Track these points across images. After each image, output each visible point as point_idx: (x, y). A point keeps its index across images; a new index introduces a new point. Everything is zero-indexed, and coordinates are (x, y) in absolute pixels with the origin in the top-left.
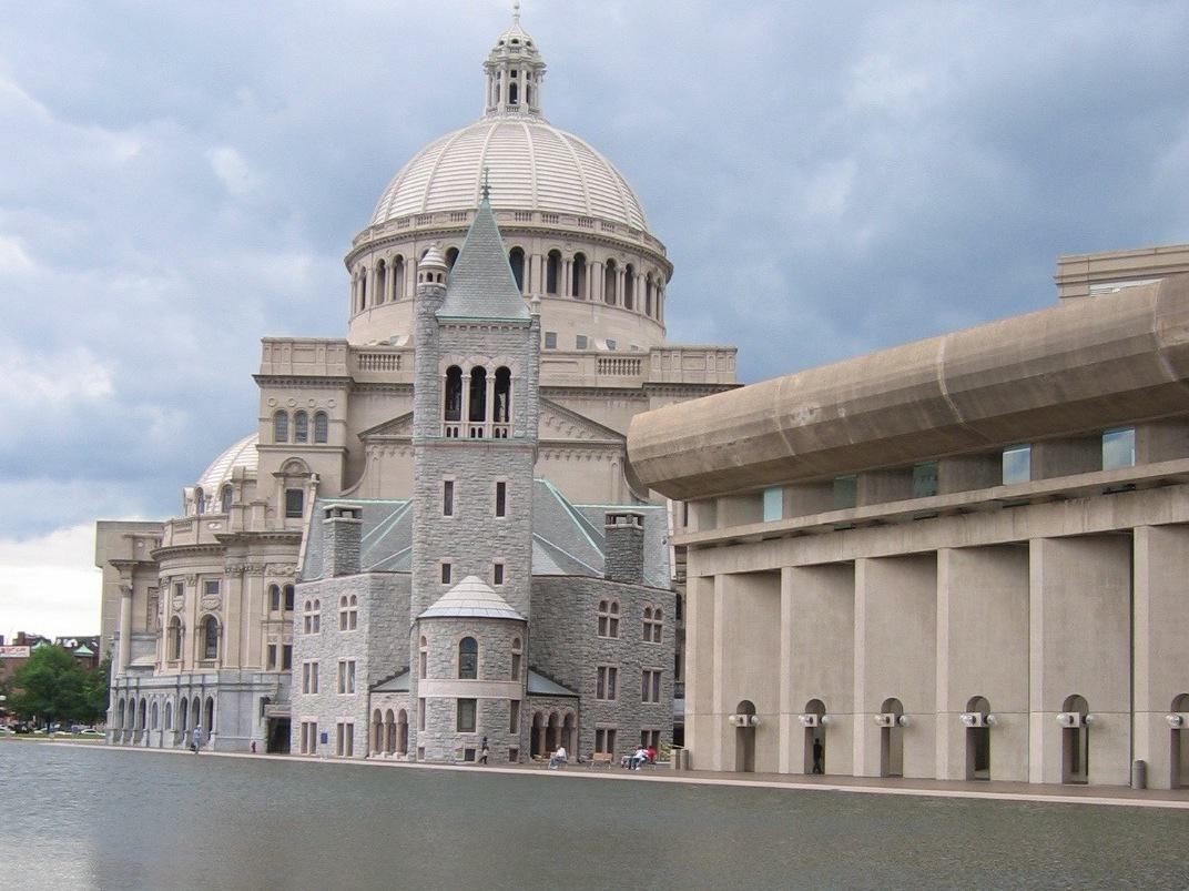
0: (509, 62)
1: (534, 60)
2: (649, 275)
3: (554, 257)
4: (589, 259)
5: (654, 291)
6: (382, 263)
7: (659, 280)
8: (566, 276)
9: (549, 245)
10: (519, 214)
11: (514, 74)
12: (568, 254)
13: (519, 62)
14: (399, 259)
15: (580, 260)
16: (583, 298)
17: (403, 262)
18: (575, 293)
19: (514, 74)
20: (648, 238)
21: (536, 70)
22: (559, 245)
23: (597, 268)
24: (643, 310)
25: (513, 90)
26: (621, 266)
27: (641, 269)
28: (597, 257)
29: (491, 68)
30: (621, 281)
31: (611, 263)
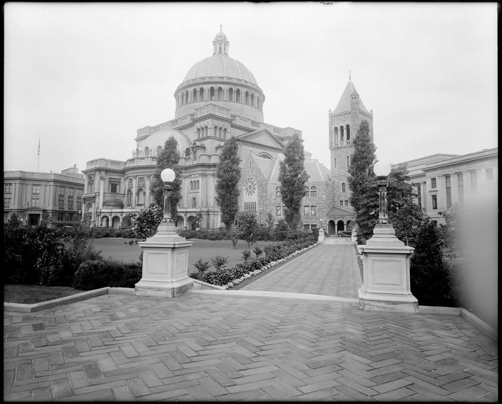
0: (219, 41)
1: (226, 41)
3: (231, 90)
4: (241, 91)
5: (259, 102)
6: (182, 94)
8: (234, 94)
9: (228, 87)
10: (220, 77)
11: (220, 45)
13: (222, 41)
14: (187, 92)
15: (238, 91)
18: (237, 101)
19: (220, 45)
20: (258, 87)
21: (227, 43)
22: (232, 87)
23: (243, 93)
24: (256, 106)
25: (220, 48)
26: (250, 93)
27: (256, 95)
29: (214, 43)
30: (250, 98)
31: (247, 93)
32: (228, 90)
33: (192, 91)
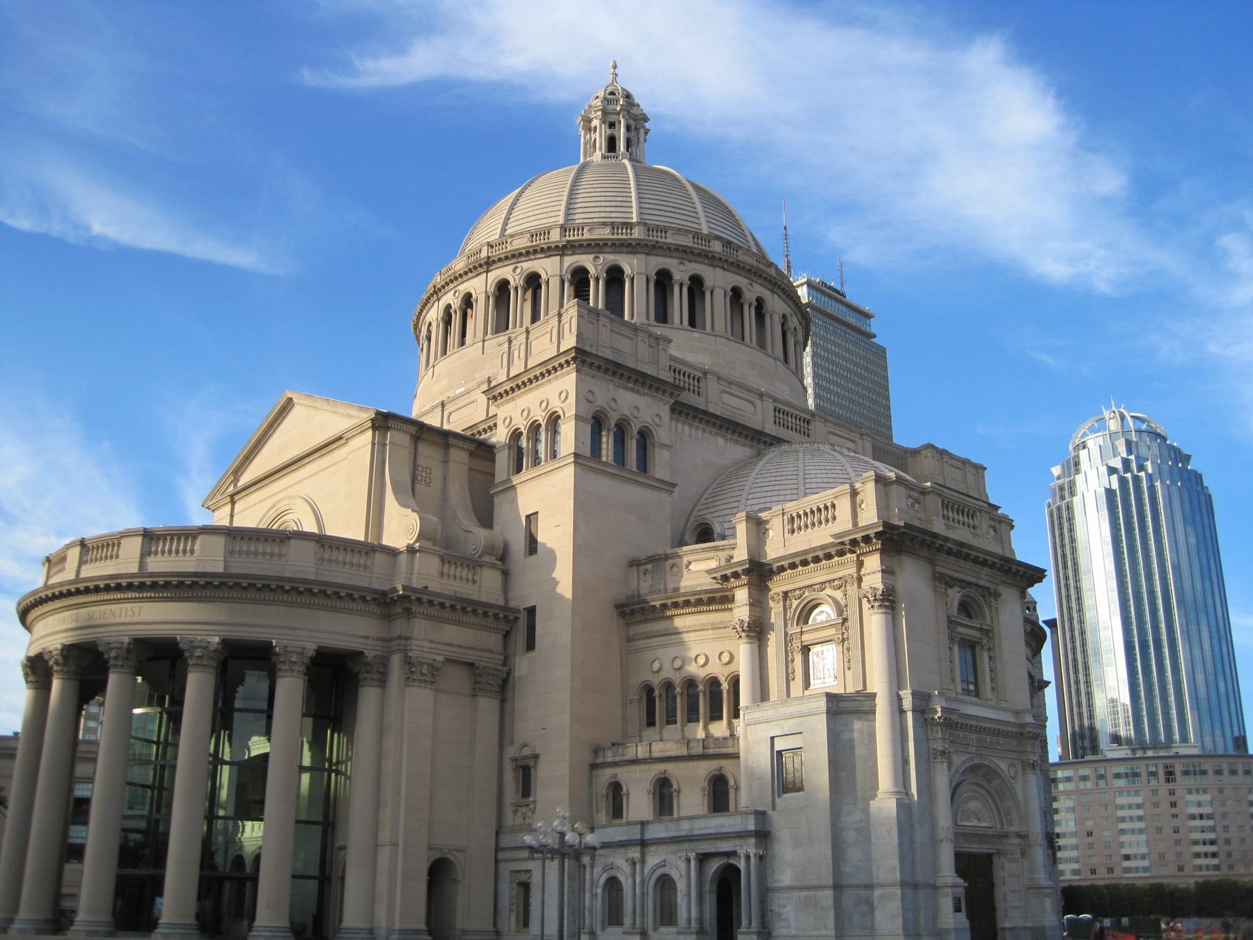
2: (784, 316)
3: (663, 281)
4: (708, 283)
6: (449, 307)
7: (795, 329)
8: (678, 302)
9: (657, 262)
11: (612, 125)
12: (681, 272)
16: (704, 328)
17: (472, 300)
18: (692, 323)
19: (612, 125)
22: (670, 263)
23: (719, 295)
28: (718, 281)
32: (653, 277)
33: (491, 289)
